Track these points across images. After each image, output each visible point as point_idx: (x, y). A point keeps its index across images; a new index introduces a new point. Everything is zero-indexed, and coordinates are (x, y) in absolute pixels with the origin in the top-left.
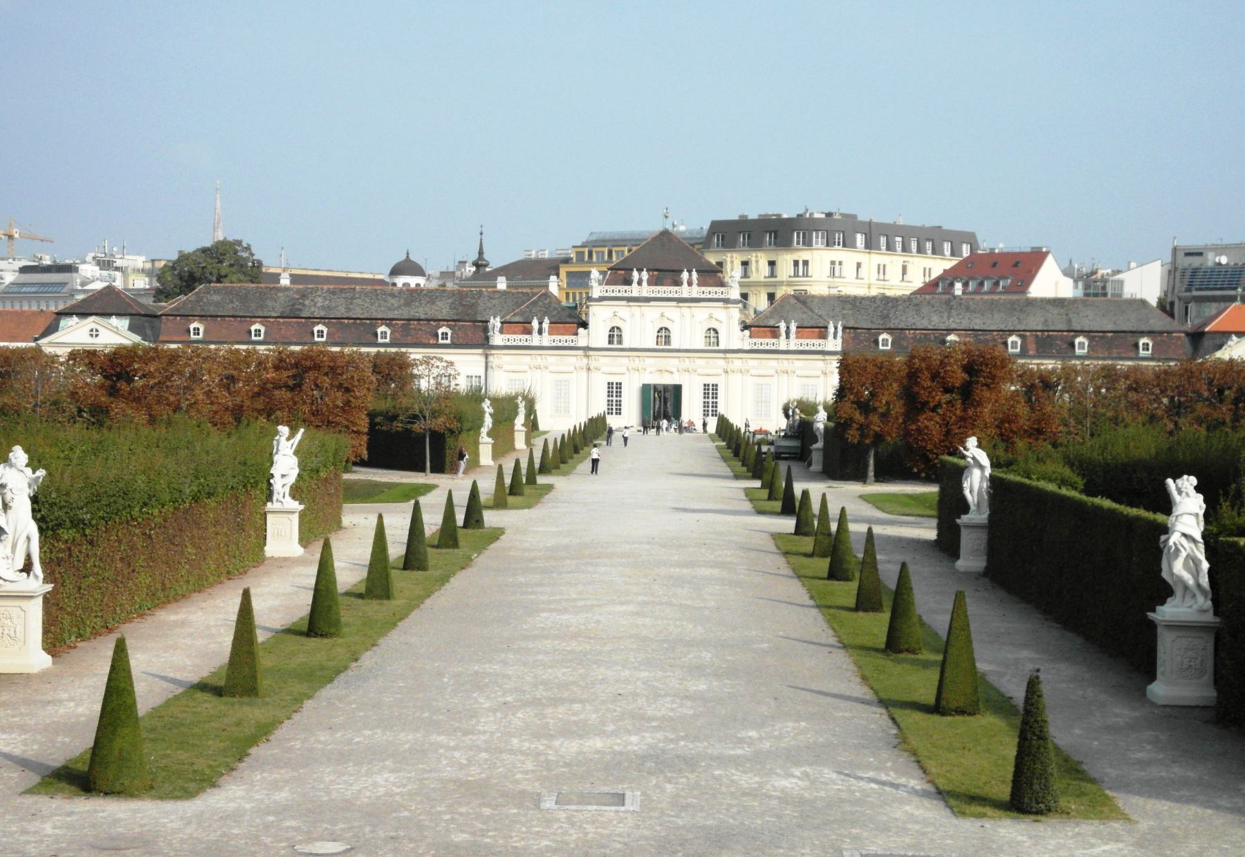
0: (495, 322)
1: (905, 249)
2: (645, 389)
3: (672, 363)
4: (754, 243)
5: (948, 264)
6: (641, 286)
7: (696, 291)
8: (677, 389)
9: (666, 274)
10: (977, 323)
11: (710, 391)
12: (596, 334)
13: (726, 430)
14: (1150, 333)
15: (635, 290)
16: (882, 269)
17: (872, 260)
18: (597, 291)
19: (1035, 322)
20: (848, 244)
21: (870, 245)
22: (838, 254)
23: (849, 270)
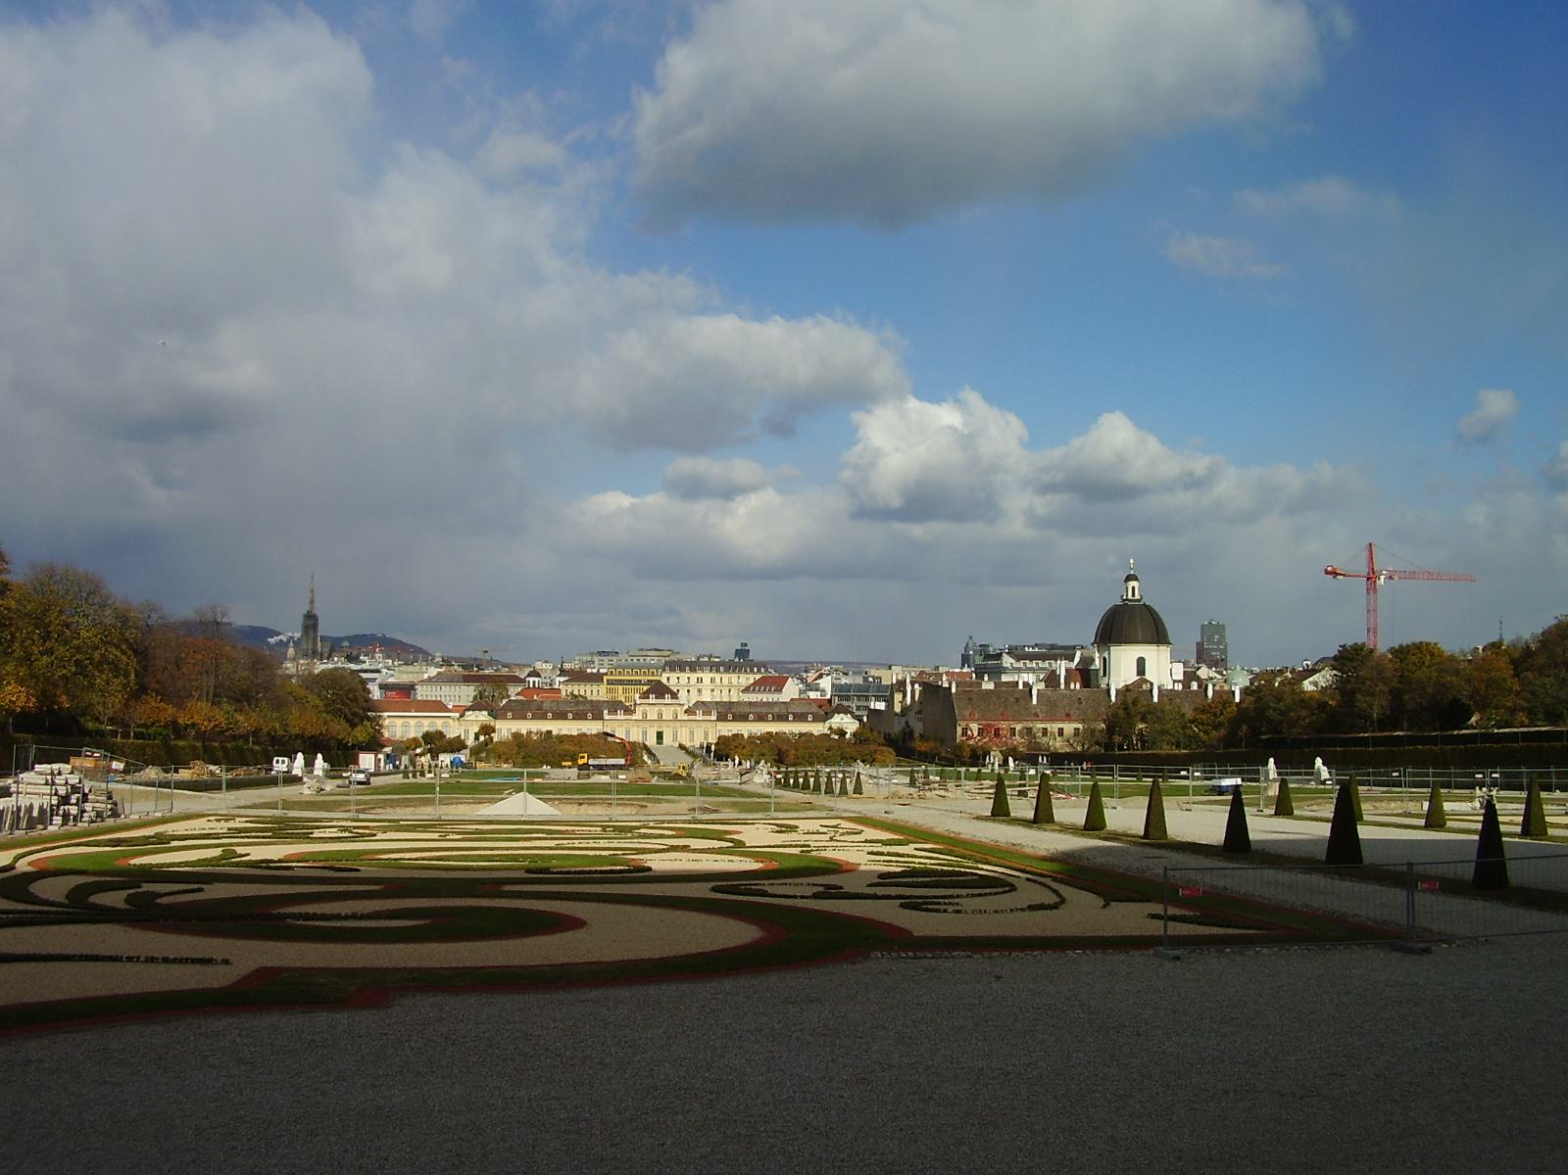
0: (606, 712)
1: (740, 672)
3: (664, 724)
4: (682, 670)
6: (652, 699)
7: (670, 701)
10: (759, 710)
11: (675, 734)
12: (638, 715)
13: (681, 747)
14: (812, 713)
15: (650, 701)
16: (730, 678)
17: (726, 677)
18: (638, 702)
19: (776, 710)
20: (718, 671)
23: (718, 681)
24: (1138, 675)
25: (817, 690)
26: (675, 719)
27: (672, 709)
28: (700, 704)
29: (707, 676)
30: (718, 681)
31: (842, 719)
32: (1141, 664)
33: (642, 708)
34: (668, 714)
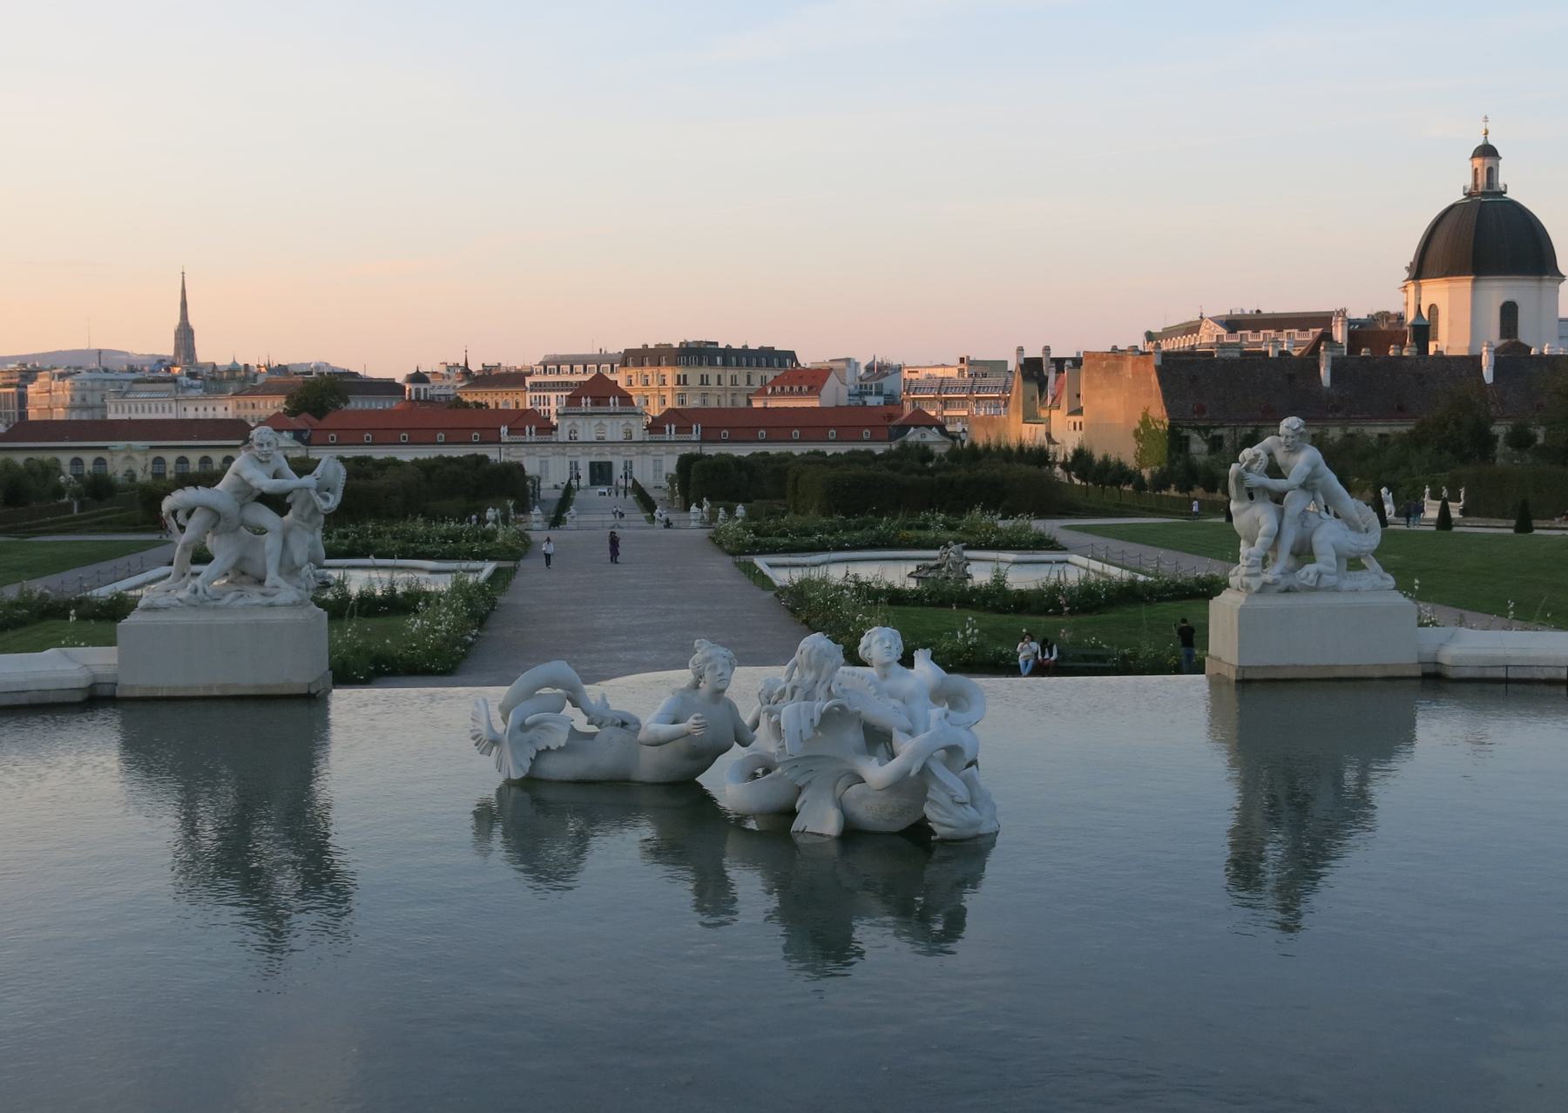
0: (504, 429)
2: (592, 464)
5: (778, 373)
8: (610, 464)
9: (599, 400)
11: (628, 467)
12: (562, 435)
17: (729, 373)
20: (712, 363)
21: (726, 364)
22: (705, 370)
23: (713, 381)
24: (1502, 336)
25: (879, 393)
26: (629, 441)
27: (623, 422)
28: (671, 415)
29: (694, 375)
30: (713, 381)
31: (923, 436)
32: (1509, 312)
33: (568, 422)
34: (614, 429)
